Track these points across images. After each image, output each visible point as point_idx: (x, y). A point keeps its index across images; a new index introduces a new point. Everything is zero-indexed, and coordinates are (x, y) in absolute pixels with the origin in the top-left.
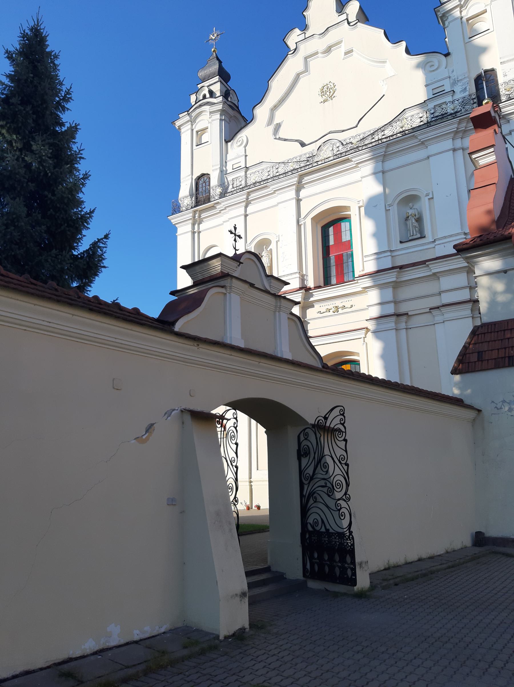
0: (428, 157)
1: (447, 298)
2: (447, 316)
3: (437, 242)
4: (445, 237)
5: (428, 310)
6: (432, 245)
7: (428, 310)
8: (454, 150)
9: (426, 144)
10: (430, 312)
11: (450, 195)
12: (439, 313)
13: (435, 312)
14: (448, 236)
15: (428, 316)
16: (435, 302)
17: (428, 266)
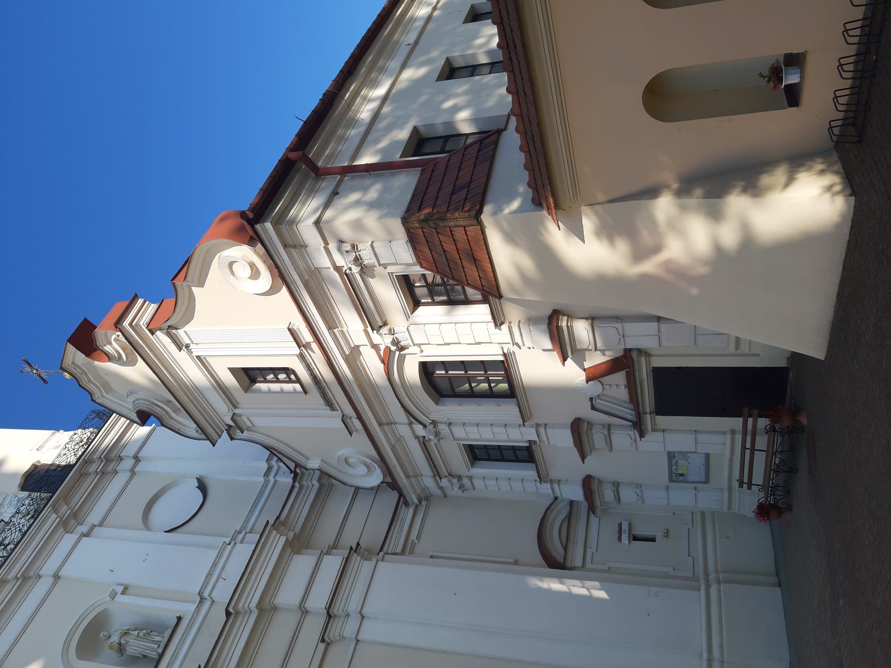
0: (57, 577)
1: (318, 600)
2: (353, 606)
3: (206, 594)
4: (209, 575)
5: (322, 646)
6: (207, 604)
7: (322, 646)
8: (87, 535)
9: (31, 573)
10: (328, 644)
11: (147, 555)
12: (340, 624)
13: (334, 632)
14: (211, 569)
15: (333, 651)
16: (314, 626)
17: (238, 613)
